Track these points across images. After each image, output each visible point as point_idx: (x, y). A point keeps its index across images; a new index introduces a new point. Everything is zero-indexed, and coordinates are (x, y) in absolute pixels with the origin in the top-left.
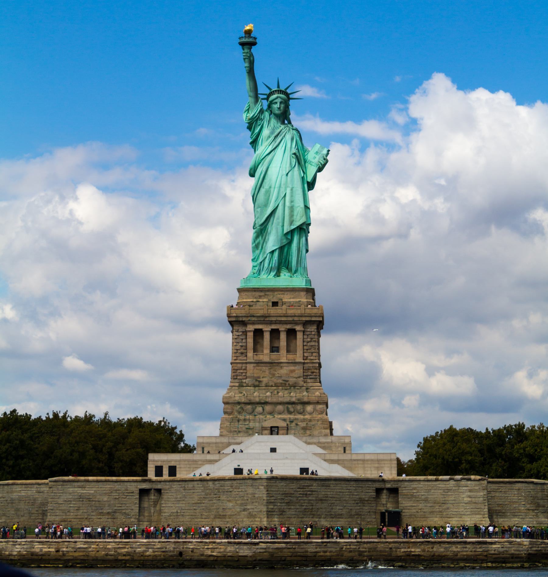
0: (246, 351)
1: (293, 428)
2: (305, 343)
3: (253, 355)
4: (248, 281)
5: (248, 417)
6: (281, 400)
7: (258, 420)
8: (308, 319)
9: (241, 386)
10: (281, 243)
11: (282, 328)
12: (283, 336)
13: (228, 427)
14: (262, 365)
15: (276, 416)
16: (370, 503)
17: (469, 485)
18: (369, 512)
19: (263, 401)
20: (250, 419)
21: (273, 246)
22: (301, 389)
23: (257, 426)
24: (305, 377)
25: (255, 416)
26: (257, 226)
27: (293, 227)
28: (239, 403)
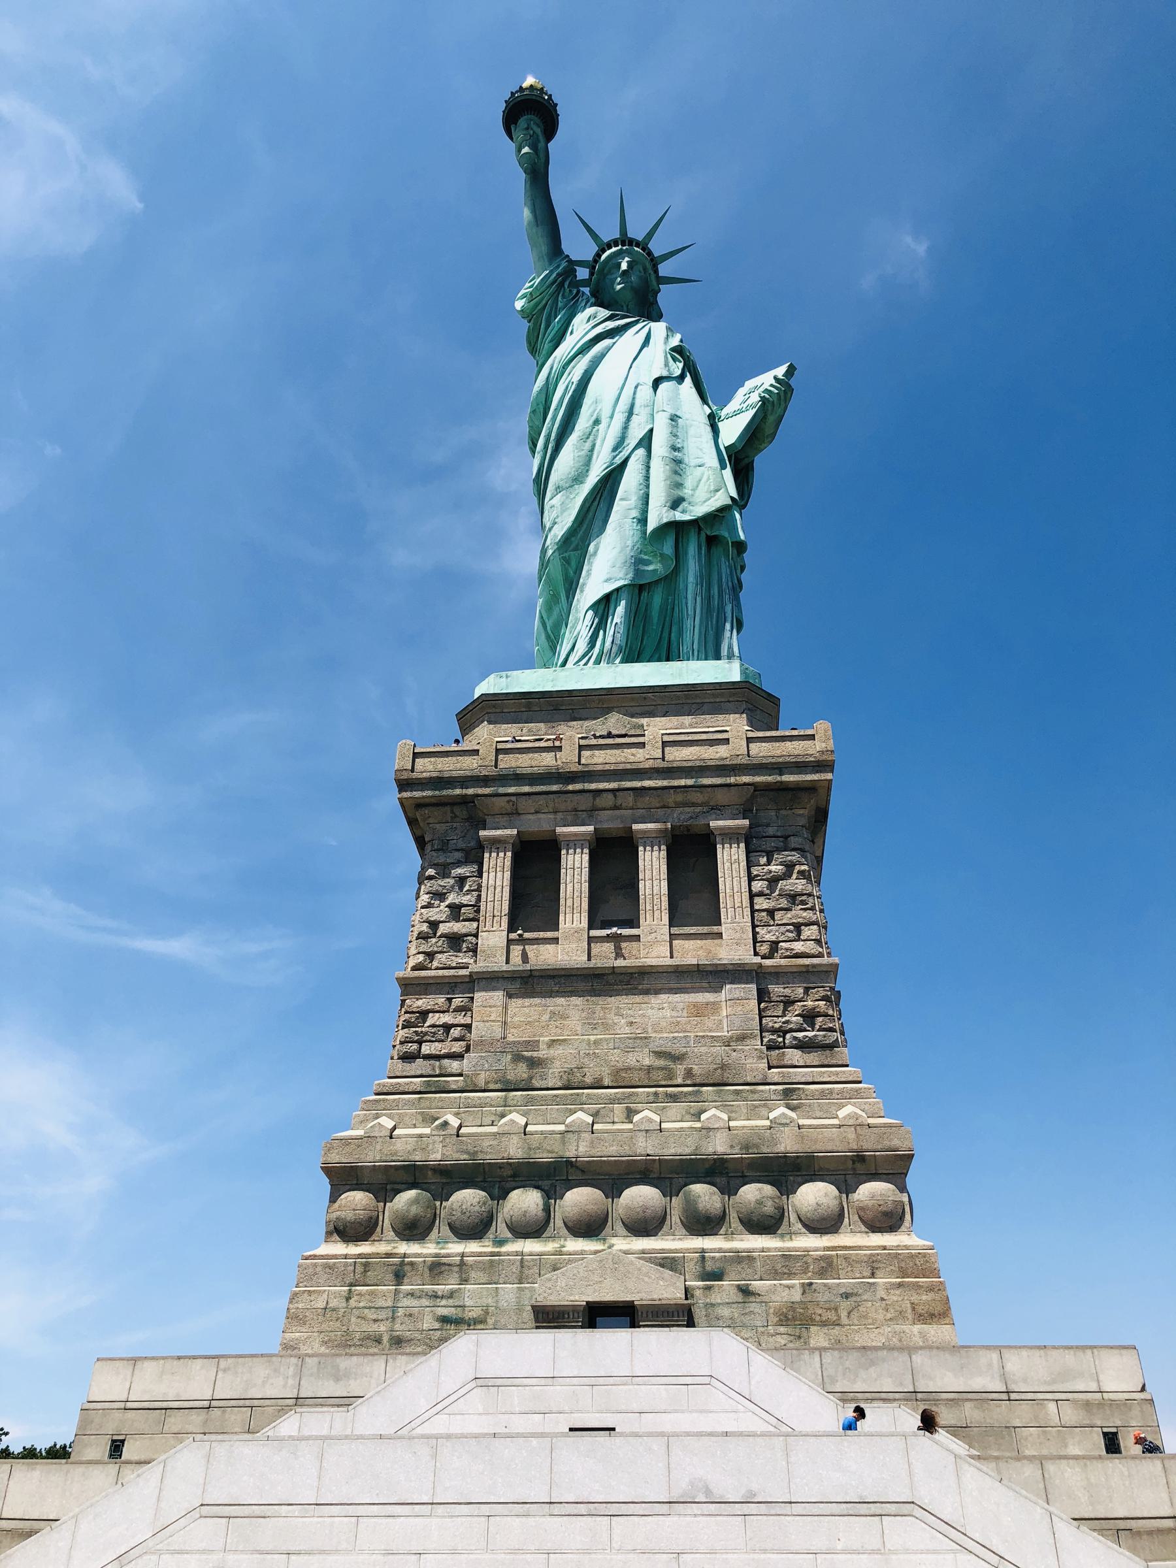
0: (475, 924)
1: (725, 1312)
2: (758, 886)
3: (510, 942)
4: (504, 679)
5: (456, 1248)
6: (645, 1147)
7: (518, 1263)
10: (638, 573)
13: (334, 1310)
15: (623, 1243)
19: (544, 1157)
21: (607, 580)
22: (753, 1092)
23: (504, 1304)
25: (500, 1242)
26: (550, 552)
27: (679, 516)
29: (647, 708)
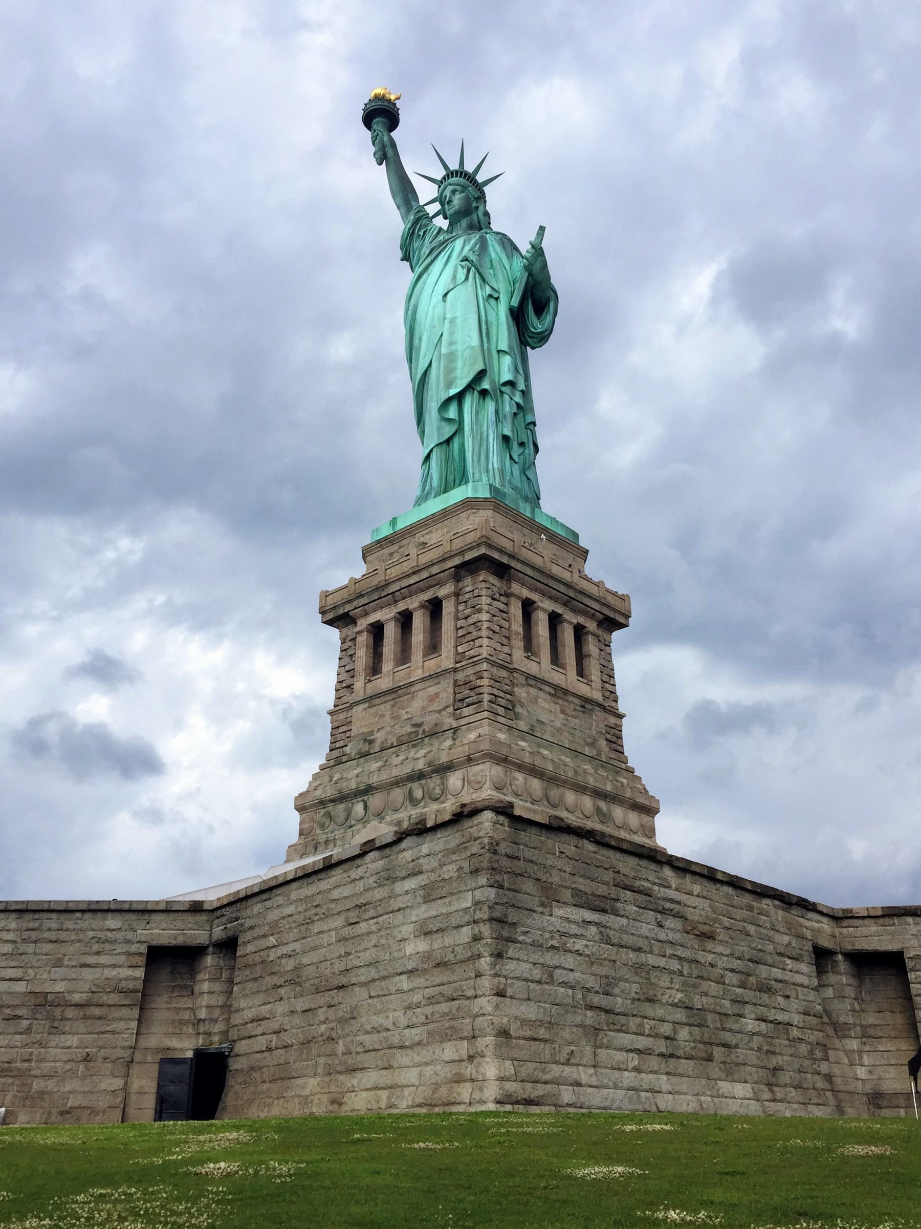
2: (460, 623)
3: (365, 684)
6: (395, 772)
8: (457, 561)
9: (338, 762)
11: (413, 603)
12: (419, 622)
14: (378, 701)
16: (100, 1018)
17: (425, 864)
18: (87, 1059)
19: (362, 787)
20: (336, 837)
24: (459, 705)
25: (351, 827)
27: (453, 392)
28: (322, 803)
29: (429, 529)
